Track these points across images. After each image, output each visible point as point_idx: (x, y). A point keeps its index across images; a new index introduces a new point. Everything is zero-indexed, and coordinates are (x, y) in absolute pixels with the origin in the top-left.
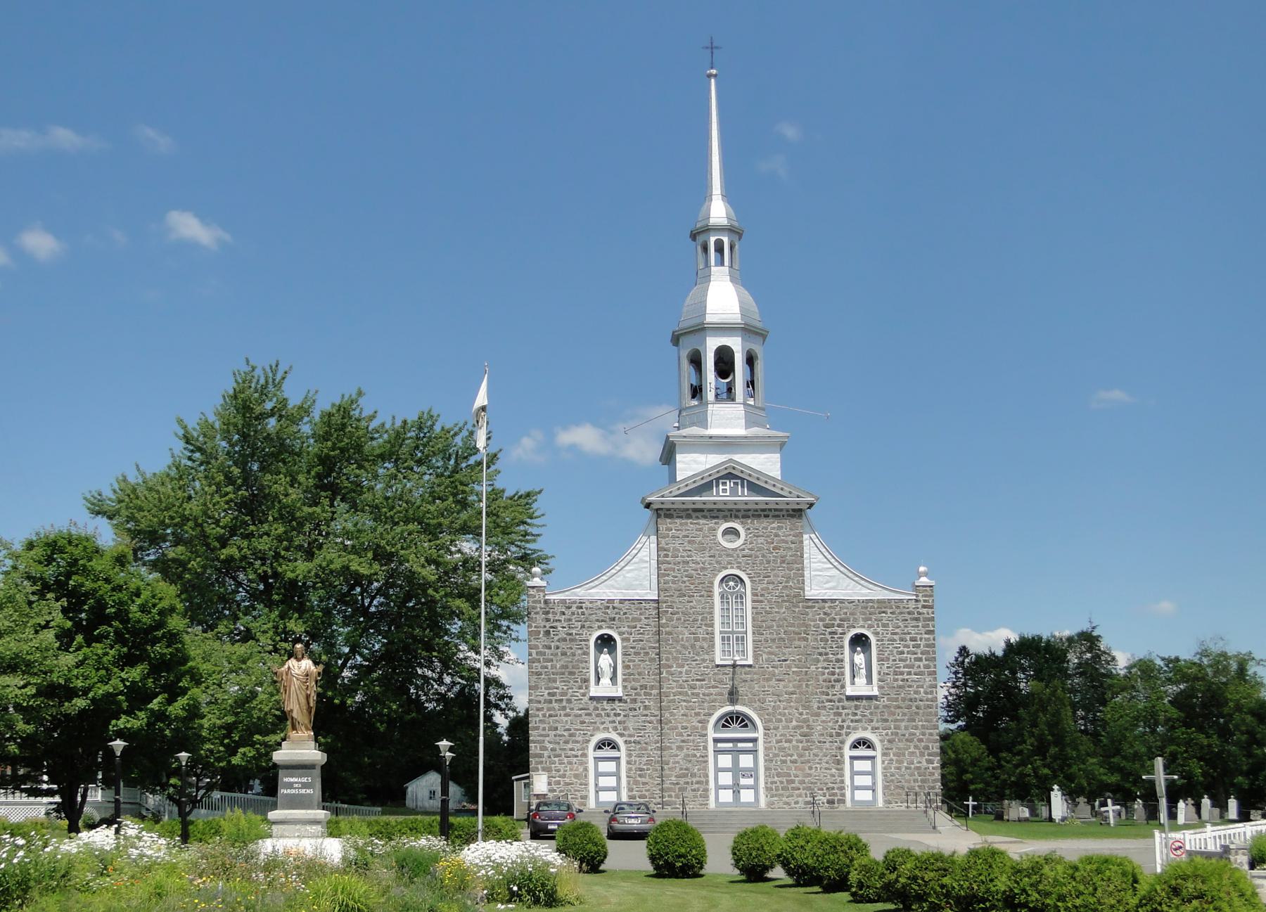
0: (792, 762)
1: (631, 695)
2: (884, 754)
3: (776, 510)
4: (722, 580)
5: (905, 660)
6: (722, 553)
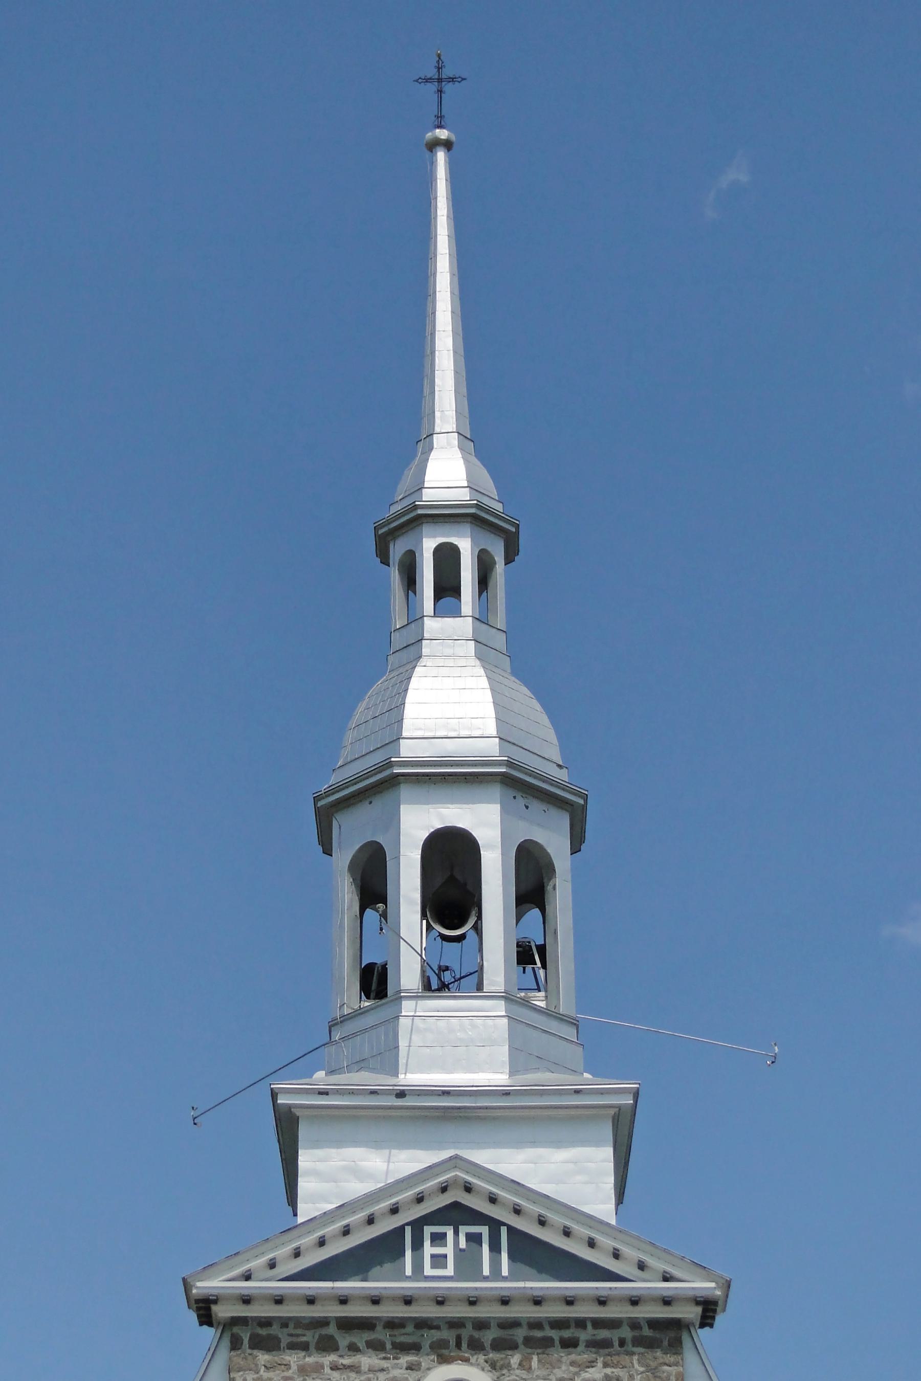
3: (598, 1323)
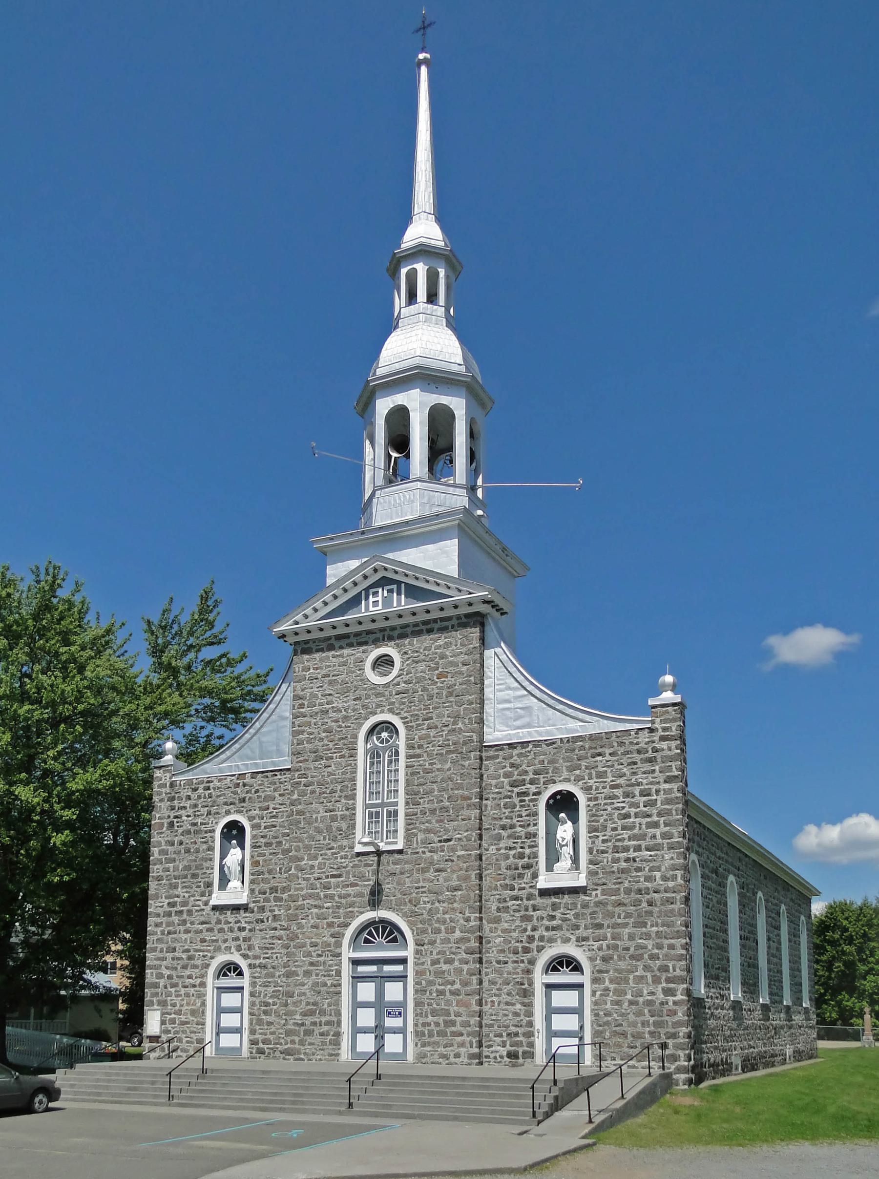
0: (453, 993)
1: (258, 902)
2: (595, 981)
3: (442, 619)
4: (371, 731)
5: (631, 828)
6: (370, 692)
